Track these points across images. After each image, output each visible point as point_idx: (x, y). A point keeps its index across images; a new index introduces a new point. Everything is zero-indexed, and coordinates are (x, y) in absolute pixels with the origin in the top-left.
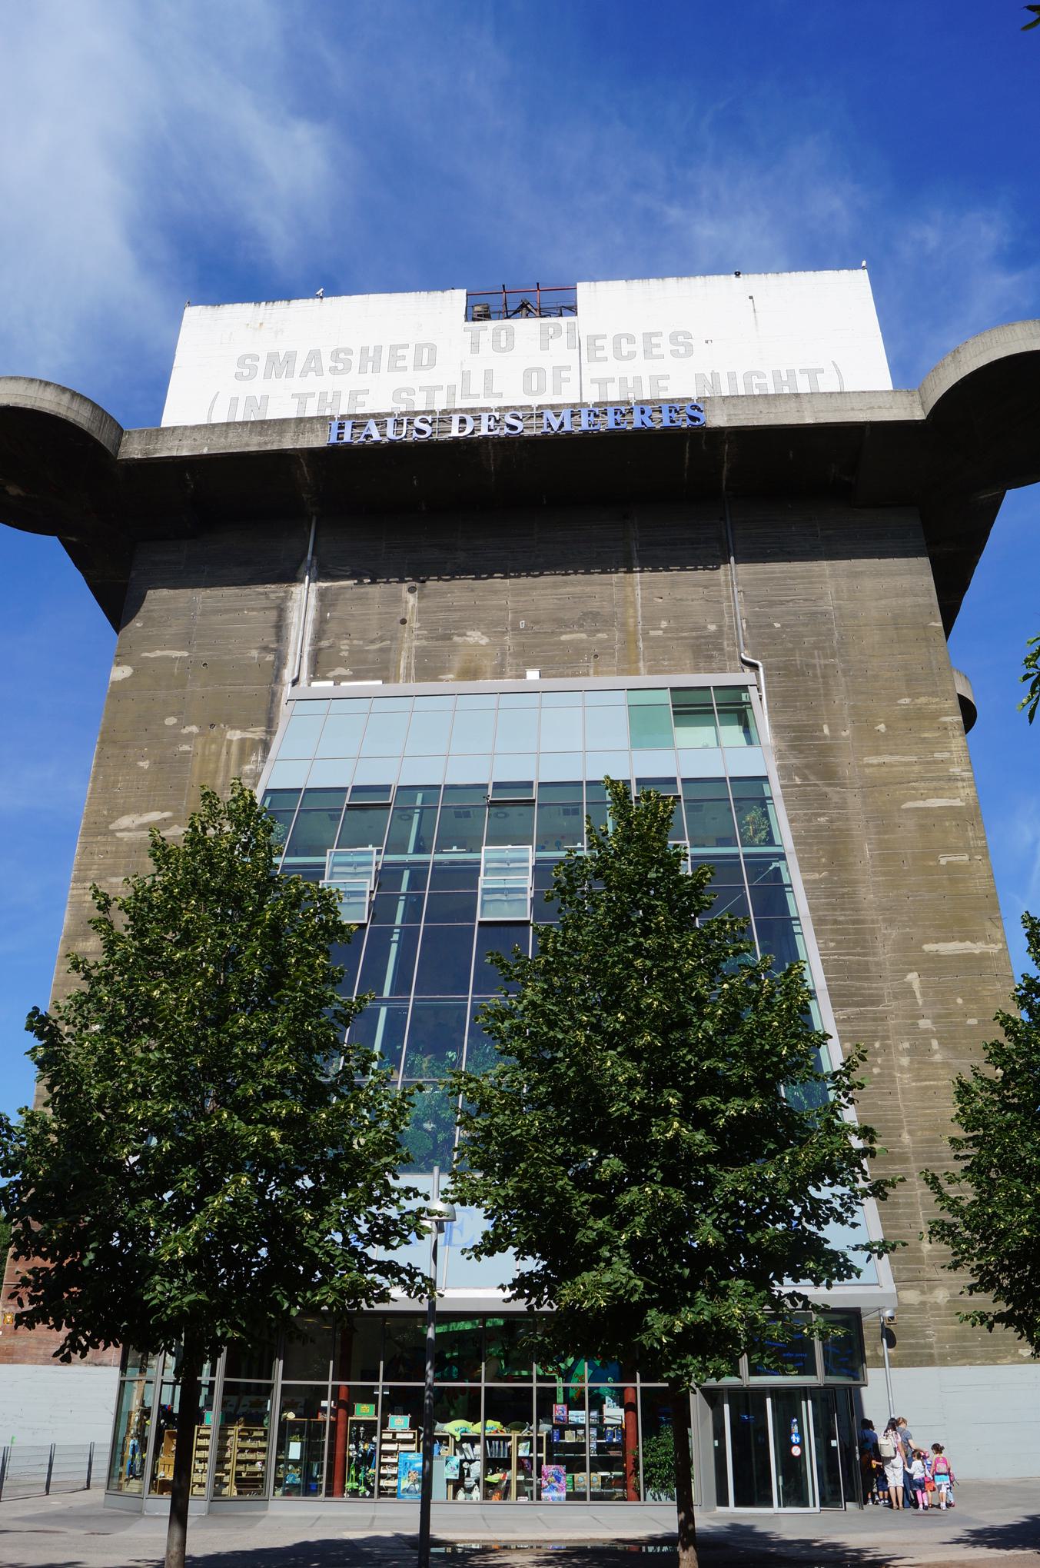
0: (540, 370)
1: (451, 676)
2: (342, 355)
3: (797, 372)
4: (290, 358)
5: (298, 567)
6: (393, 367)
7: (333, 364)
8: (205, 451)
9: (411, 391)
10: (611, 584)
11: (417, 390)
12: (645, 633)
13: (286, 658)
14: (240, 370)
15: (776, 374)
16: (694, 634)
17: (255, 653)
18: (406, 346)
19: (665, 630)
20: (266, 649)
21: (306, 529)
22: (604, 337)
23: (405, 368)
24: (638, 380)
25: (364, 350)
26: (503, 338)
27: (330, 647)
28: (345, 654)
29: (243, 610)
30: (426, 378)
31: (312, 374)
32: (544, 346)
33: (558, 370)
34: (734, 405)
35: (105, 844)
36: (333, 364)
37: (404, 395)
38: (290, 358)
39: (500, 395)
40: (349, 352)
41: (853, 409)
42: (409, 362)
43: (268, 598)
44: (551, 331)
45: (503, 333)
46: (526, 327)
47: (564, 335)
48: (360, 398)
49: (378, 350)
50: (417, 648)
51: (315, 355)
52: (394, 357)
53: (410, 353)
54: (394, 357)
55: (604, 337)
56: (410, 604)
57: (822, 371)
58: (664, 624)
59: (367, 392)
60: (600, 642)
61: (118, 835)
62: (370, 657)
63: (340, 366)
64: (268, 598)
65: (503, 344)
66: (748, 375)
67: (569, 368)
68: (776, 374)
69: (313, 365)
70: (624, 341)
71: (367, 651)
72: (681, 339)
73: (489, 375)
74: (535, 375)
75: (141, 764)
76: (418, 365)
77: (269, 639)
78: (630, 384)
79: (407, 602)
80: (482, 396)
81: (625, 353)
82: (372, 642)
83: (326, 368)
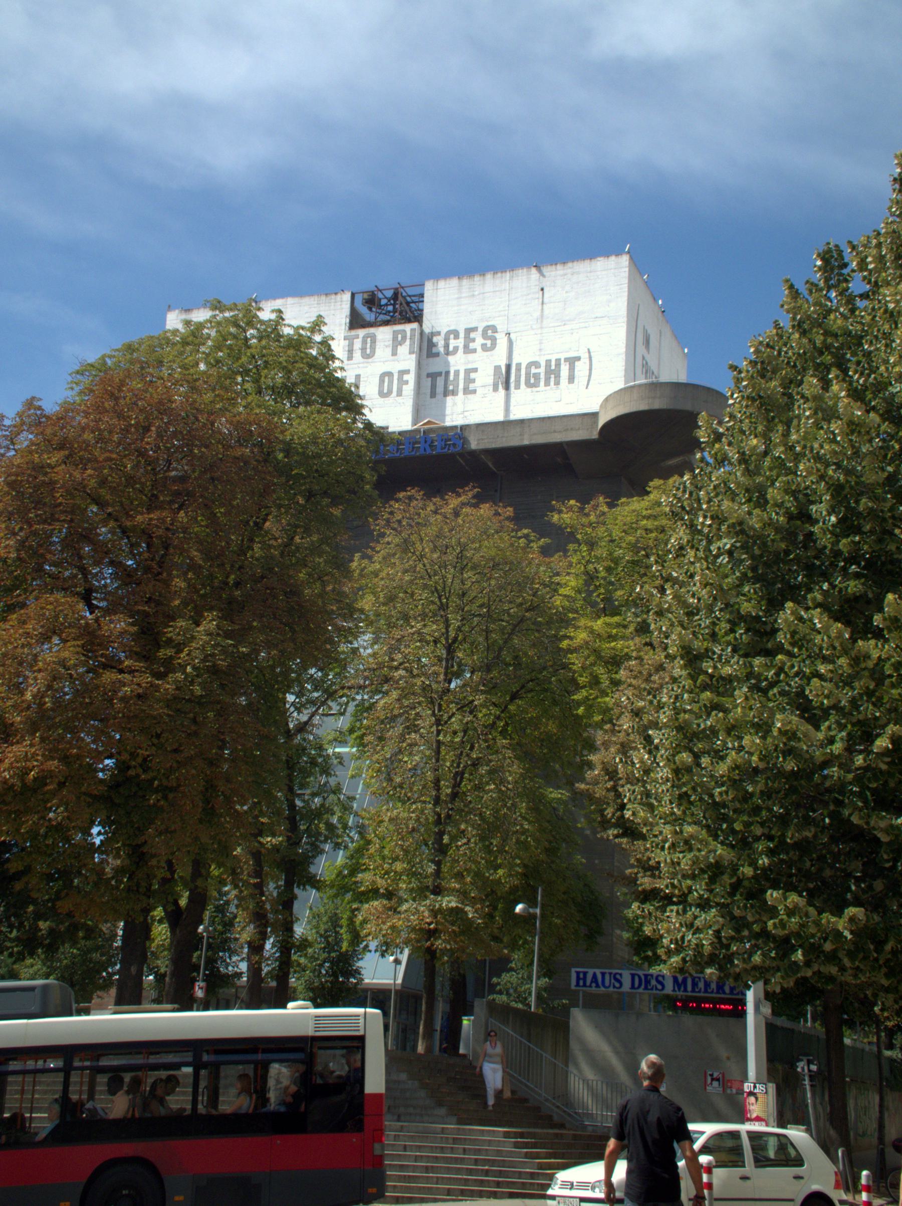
0: (389, 374)
15: (548, 362)
22: (439, 333)
24: (457, 373)
26: (368, 345)
32: (394, 353)
33: (402, 373)
34: (483, 431)
41: (555, 432)
44: (400, 336)
45: (369, 339)
47: (408, 342)
57: (578, 359)
67: (407, 372)
70: (452, 336)
72: (490, 332)
74: (386, 379)
78: (452, 377)
81: (451, 349)
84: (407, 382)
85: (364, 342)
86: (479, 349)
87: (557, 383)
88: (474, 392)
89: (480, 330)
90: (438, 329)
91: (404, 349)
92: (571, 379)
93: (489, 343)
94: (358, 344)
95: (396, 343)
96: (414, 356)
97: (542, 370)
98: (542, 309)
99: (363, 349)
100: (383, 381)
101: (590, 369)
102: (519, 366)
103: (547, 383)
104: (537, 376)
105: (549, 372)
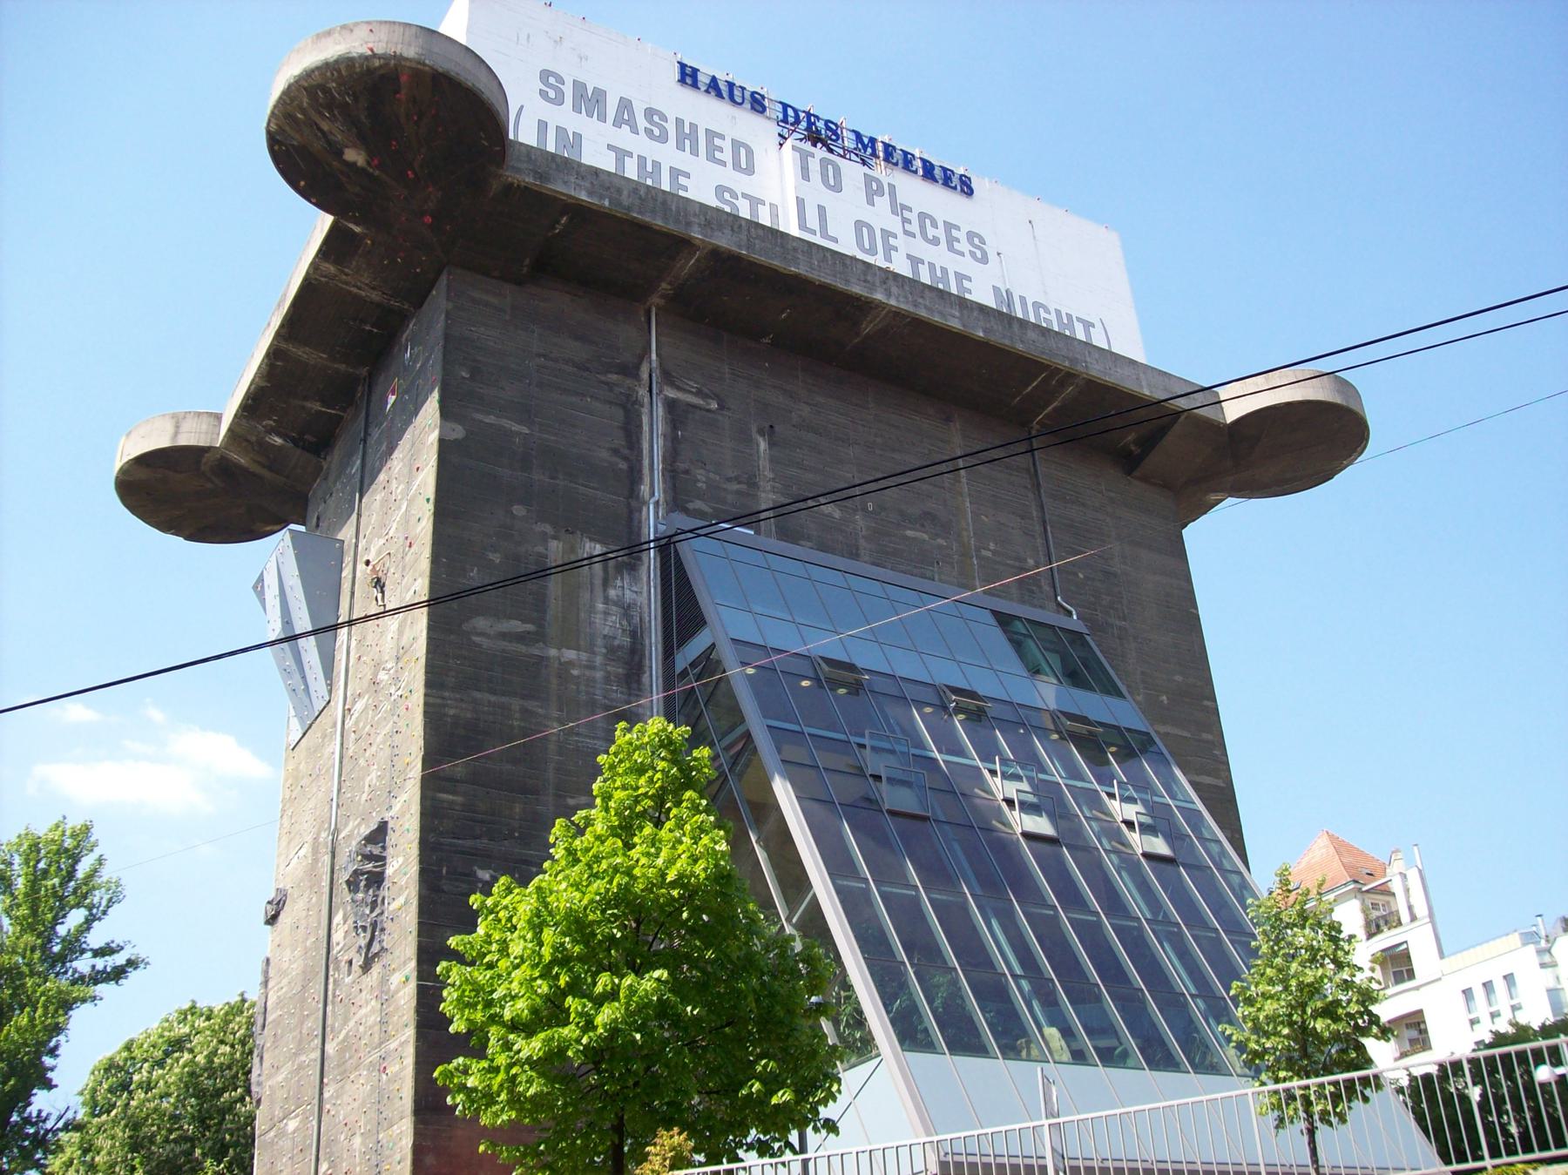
1: (809, 544)
4: (599, 97)
6: (711, 157)
10: (944, 488)
12: (978, 550)
13: (640, 471)
16: (1017, 564)
17: (604, 454)
19: (994, 552)
20: (616, 452)
23: (724, 164)
28: (704, 486)
29: (584, 395)
30: (739, 183)
42: (727, 156)
43: (611, 390)
47: (887, 195)
53: (727, 145)
58: (992, 546)
60: (940, 547)
62: (730, 498)
64: (611, 390)
65: (832, 182)
68: (1058, 312)
69: (626, 117)
73: (822, 210)
75: (491, 556)
77: (619, 441)
79: (758, 445)
80: (818, 234)
82: (729, 480)
83: (642, 132)
84: (896, 249)
86: (967, 254)
89: (964, 230)
94: (814, 165)
98: (1036, 245)
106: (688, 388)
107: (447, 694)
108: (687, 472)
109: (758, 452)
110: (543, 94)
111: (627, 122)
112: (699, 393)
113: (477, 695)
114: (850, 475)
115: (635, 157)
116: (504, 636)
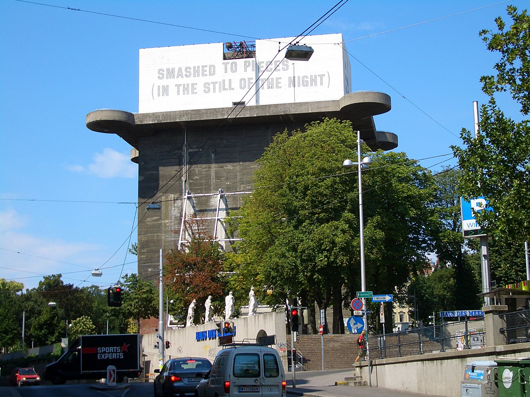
0: (244, 79)
2: (188, 70)
3: (317, 76)
4: (173, 69)
5: (183, 145)
6: (203, 75)
7: (186, 73)
8: (156, 122)
9: (209, 84)
11: (210, 83)
14: (159, 75)
15: (311, 76)
18: (206, 66)
21: (184, 133)
25: (194, 67)
27: (193, 170)
28: (197, 172)
31: (180, 77)
32: (245, 71)
33: (249, 79)
35: (144, 225)
36: (186, 73)
37: (207, 85)
38: (173, 69)
39: (233, 89)
40: (190, 68)
42: (207, 73)
44: (247, 64)
45: (234, 65)
46: (240, 62)
48: (195, 86)
49: (198, 67)
50: (215, 170)
51: (180, 69)
52: (204, 71)
53: (207, 69)
54: (204, 71)
55: (263, 62)
56: (213, 157)
57: (324, 75)
59: (196, 84)
61: (147, 223)
62: (204, 173)
63: (188, 74)
66: (304, 77)
67: (252, 79)
69: (180, 74)
71: (203, 171)
73: (230, 80)
74: (243, 81)
76: (210, 74)
79: (212, 156)
85: (232, 65)
86: (281, 70)
87: (316, 85)
88: (281, 87)
90: (262, 61)
91: (250, 69)
92: (322, 84)
93: (285, 67)
94: (229, 66)
95: (246, 66)
96: (254, 72)
97: (309, 79)
99: (232, 68)
100: (242, 82)
101: (329, 80)
102: (299, 77)
103: (312, 85)
104: (307, 82)
105: (312, 80)
106: (194, 147)
107: (142, 236)
108: (193, 170)
109: (212, 158)
110: (159, 78)
111: (180, 75)
112: (198, 148)
113: (148, 235)
114: (236, 156)
115: (182, 85)
116: (153, 221)
